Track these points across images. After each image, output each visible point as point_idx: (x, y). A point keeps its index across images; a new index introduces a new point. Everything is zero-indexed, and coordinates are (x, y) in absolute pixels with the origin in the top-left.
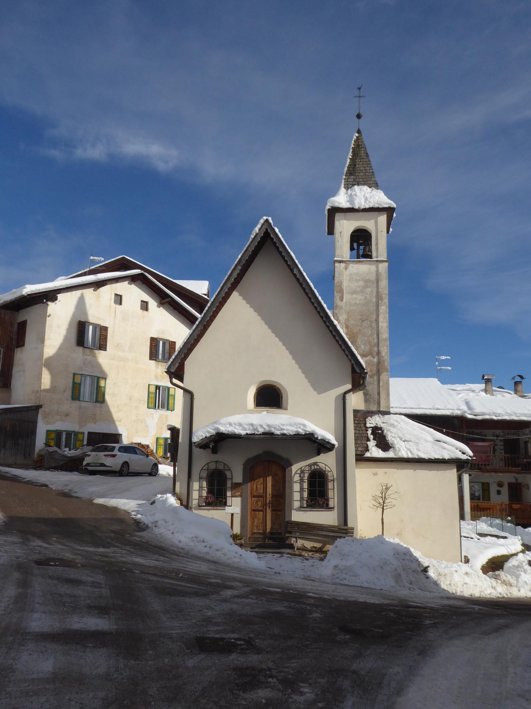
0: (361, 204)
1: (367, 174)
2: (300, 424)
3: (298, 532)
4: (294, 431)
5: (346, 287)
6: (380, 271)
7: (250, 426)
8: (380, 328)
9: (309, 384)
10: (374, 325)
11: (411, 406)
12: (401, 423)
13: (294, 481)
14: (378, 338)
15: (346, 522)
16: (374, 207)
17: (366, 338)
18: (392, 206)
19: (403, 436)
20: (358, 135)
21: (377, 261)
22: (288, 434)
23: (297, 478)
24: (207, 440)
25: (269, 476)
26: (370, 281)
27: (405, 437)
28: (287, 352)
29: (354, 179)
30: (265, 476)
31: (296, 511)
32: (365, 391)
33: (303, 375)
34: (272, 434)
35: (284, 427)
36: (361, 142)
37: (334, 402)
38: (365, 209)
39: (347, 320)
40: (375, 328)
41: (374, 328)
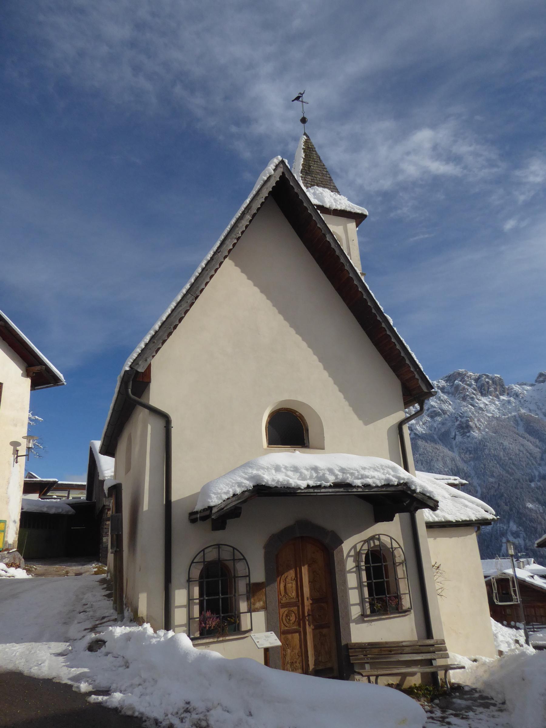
1: (325, 178)
3: (367, 663)
4: (382, 479)
7: (313, 472)
9: (351, 408)
13: (347, 569)
15: (429, 634)
16: (346, 209)
18: (365, 213)
23: (350, 564)
24: (236, 500)
25: (304, 565)
28: (315, 358)
30: (297, 567)
31: (356, 624)
33: (341, 396)
34: (349, 486)
35: (366, 473)
36: (311, 145)
37: (387, 437)
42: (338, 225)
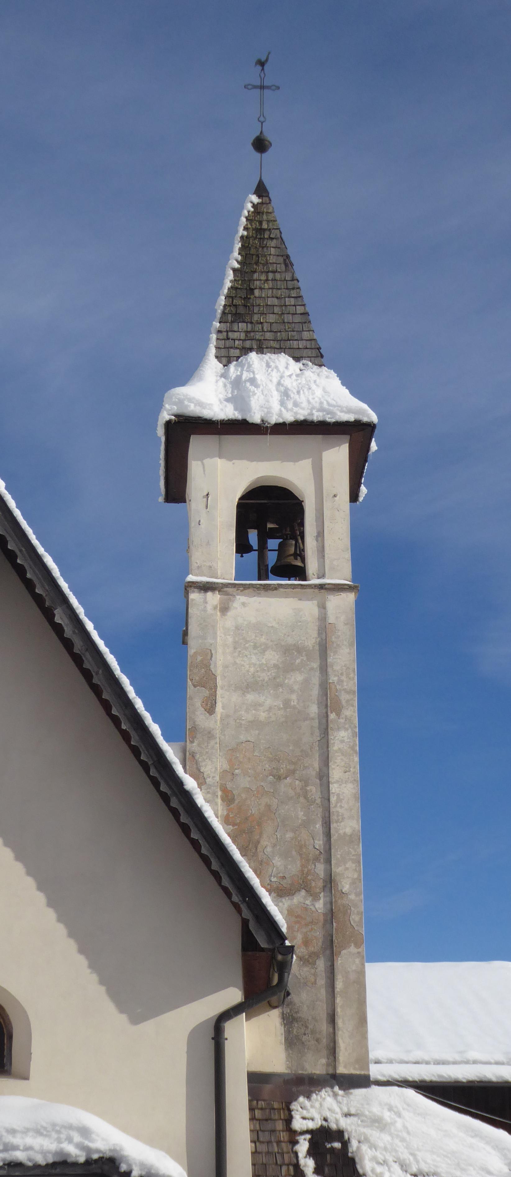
0: (269, 408)
1: (288, 318)
2: (71, 1127)
4: (49, 1152)
5: (226, 667)
6: (331, 619)
8: (333, 799)
9: (103, 989)
10: (314, 791)
11: (437, 1056)
12: (405, 1114)
14: (328, 834)
16: (310, 418)
17: (289, 835)
18: (365, 419)
19: (411, 1158)
20: (260, 201)
21: (321, 587)
22: (30, 1164)
26: (299, 649)
27: (417, 1162)
28: (30, 882)
29: (247, 332)
32: (287, 1010)
33: (82, 961)
35: (17, 1140)
36: (268, 221)
37: (185, 1048)
38: (284, 424)
39: (228, 774)
40: (318, 801)
41: (313, 801)
42: (295, 459)
